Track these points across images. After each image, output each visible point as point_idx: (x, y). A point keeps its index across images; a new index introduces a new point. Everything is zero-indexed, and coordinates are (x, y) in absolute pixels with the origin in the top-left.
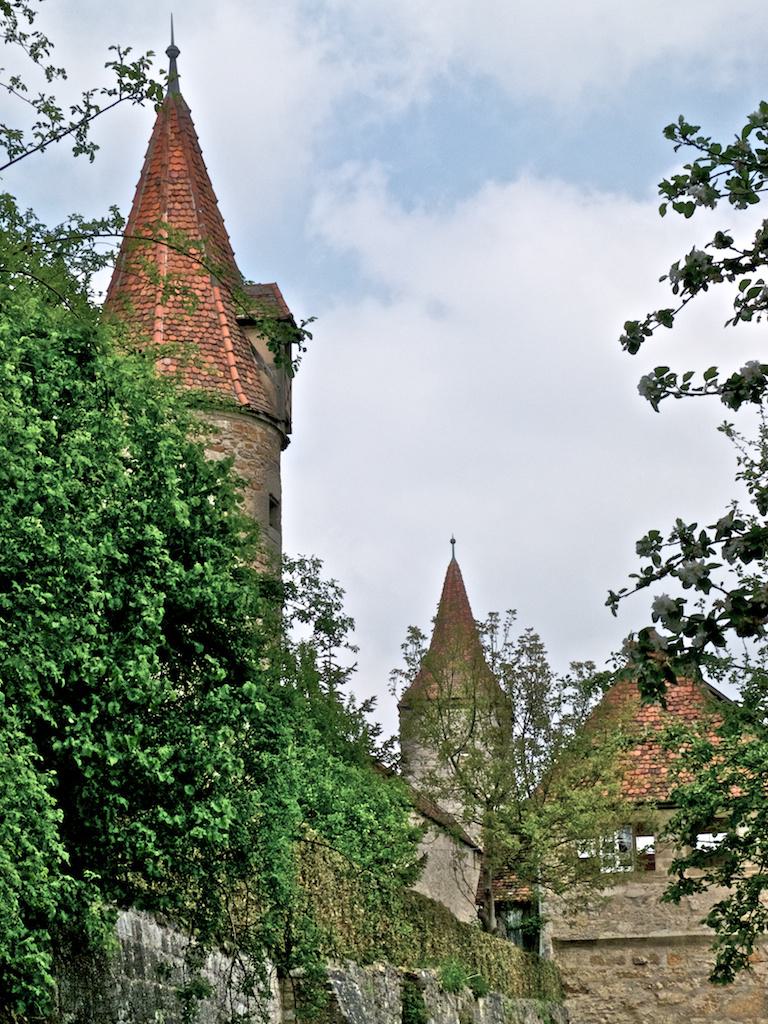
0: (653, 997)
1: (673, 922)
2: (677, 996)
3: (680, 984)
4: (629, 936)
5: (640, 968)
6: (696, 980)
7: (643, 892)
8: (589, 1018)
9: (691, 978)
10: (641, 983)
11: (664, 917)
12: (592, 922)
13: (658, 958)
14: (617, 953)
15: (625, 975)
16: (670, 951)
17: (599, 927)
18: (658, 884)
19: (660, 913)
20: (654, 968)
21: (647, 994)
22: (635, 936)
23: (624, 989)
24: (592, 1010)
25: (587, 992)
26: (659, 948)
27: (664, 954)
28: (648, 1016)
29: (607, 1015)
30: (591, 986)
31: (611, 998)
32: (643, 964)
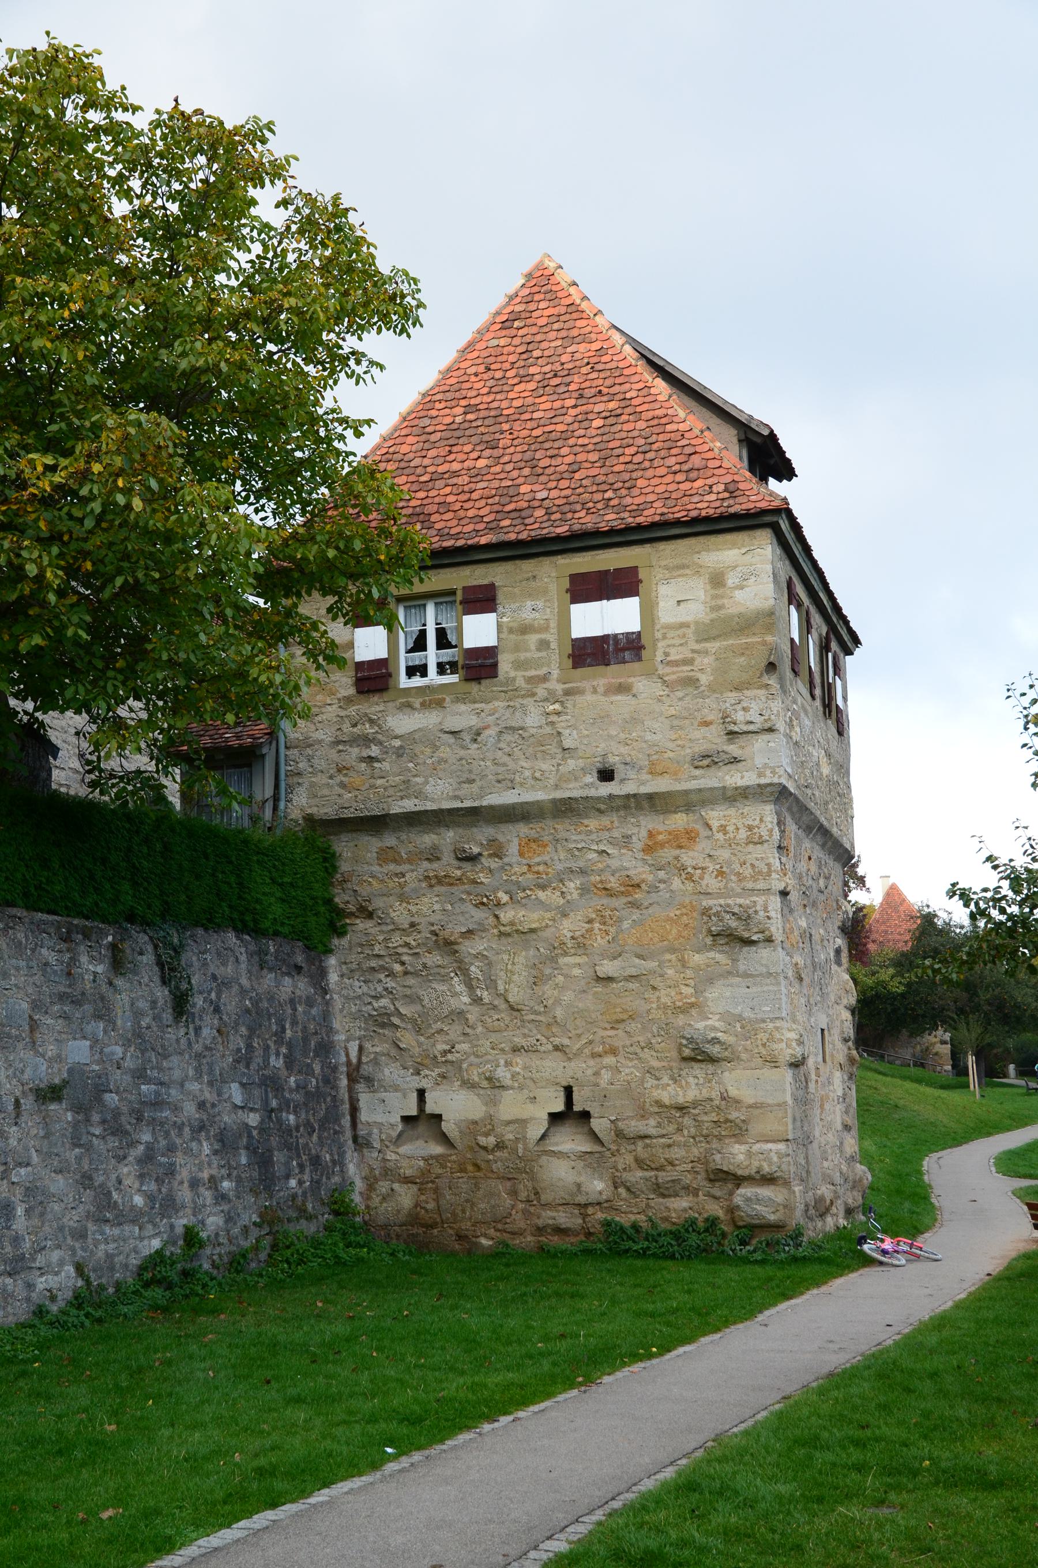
0: (491, 920)
1: (527, 773)
2: (535, 916)
3: (541, 895)
4: (447, 805)
5: (467, 866)
6: (572, 885)
7: (474, 721)
8: (373, 963)
9: (561, 881)
10: (469, 893)
11: (511, 765)
12: (379, 782)
13: (501, 846)
14: (428, 839)
15: (440, 881)
16: (523, 829)
17: (391, 791)
18: (501, 704)
19: (506, 759)
20: (494, 864)
21: (479, 914)
22: (458, 804)
23: (437, 907)
24: (378, 949)
25: (370, 915)
26: (504, 828)
27: (512, 836)
28: (479, 956)
29: (405, 958)
30: (378, 903)
31: (412, 925)
32: (473, 859)
